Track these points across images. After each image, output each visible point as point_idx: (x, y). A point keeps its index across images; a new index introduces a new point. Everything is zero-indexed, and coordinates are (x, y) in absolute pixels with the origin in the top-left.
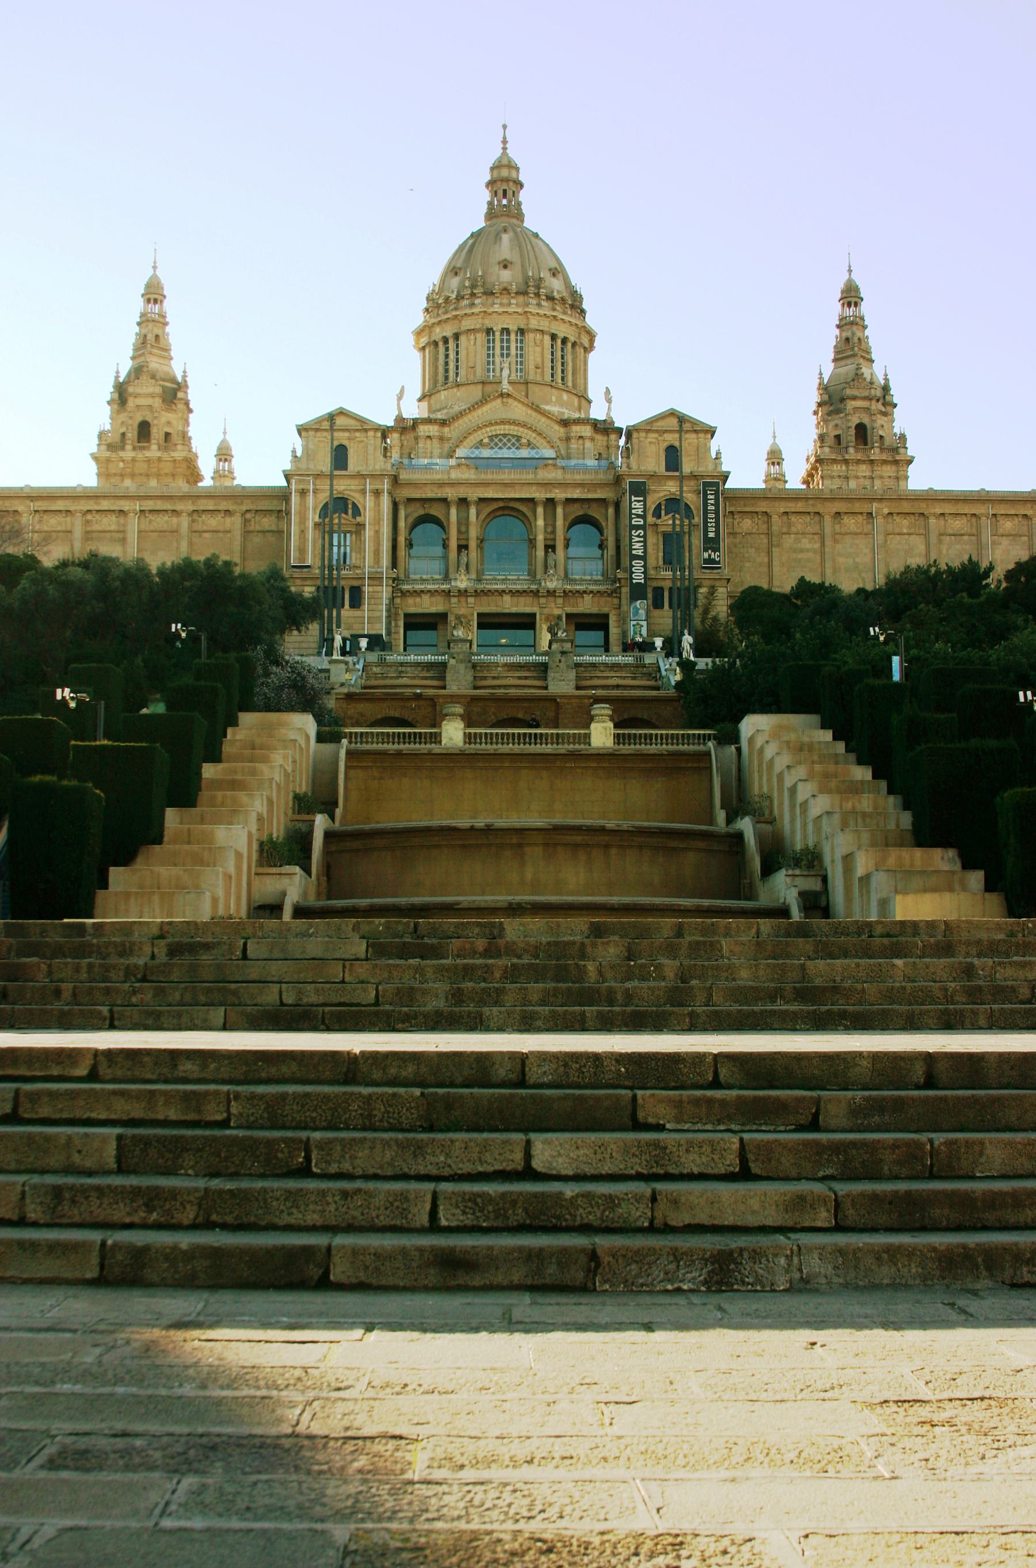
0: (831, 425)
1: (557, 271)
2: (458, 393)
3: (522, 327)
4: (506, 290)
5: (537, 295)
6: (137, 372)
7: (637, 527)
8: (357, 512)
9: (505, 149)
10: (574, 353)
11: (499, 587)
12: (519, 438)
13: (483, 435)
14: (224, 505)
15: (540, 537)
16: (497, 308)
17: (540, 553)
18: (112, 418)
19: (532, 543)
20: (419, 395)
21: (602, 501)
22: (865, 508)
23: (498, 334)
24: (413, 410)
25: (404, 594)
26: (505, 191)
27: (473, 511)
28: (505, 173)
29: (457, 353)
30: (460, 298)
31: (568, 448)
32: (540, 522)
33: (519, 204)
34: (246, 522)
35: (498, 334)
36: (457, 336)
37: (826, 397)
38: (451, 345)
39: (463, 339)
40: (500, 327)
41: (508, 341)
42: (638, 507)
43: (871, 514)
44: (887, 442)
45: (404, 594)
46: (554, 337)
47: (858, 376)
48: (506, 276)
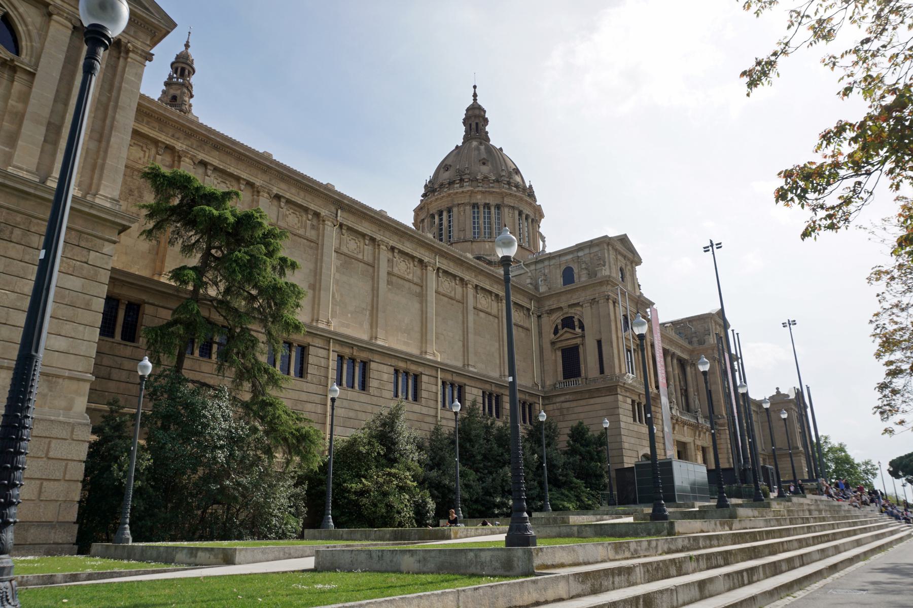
1: (517, 171)
3: (498, 202)
4: (486, 178)
5: (509, 183)
9: (475, 100)
16: (480, 189)
23: (482, 208)
26: (477, 124)
28: (477, 112)
29: (450, 222)
33: (487, 133)
35: (482, 208)
36: (449, 210)
38: (445, 214)
39: (455, 210)
40: (483, 201)
41: (489, 213)
46: (520, 213)
48: (485, 169)
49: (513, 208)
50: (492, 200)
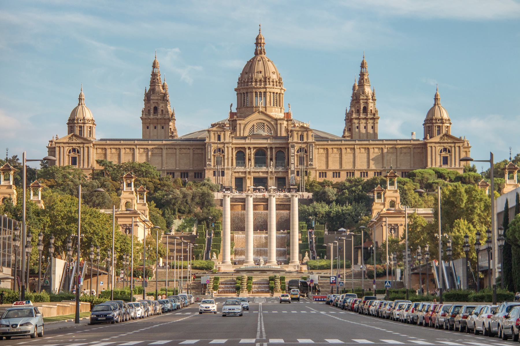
0: (356, 106)
2: (248, 109)
5: (269, 82)
6: (153, 90)
7: (293, 156)
8: (223, 152)
10: (279, 96)
11: (258, 170)
12: (264, 124)
13: (254, 123)
14: (187, 147)
15: (269, 157)
16: (258, 86)
17: (269, 161)
18: (145, 104)
19: (267, 158)
20: (236, 107)
21: (284, 148)
22: (353, 147)
24: (234, 110)
25: (235, 172)
27: (252, 150)
30: (248, 82)
31: (277, 127)
32: (269, 153)
34: (194, 151)
36: (247, 93)
37: (355, 98)
38: (245, 95)
39: (249, 94)
42: (292, 151)
43: (354, 148)
44: (373, 112)
45: (235, 172)
47: (364, 93)
49: (270, 92)
50: (263, 90)
